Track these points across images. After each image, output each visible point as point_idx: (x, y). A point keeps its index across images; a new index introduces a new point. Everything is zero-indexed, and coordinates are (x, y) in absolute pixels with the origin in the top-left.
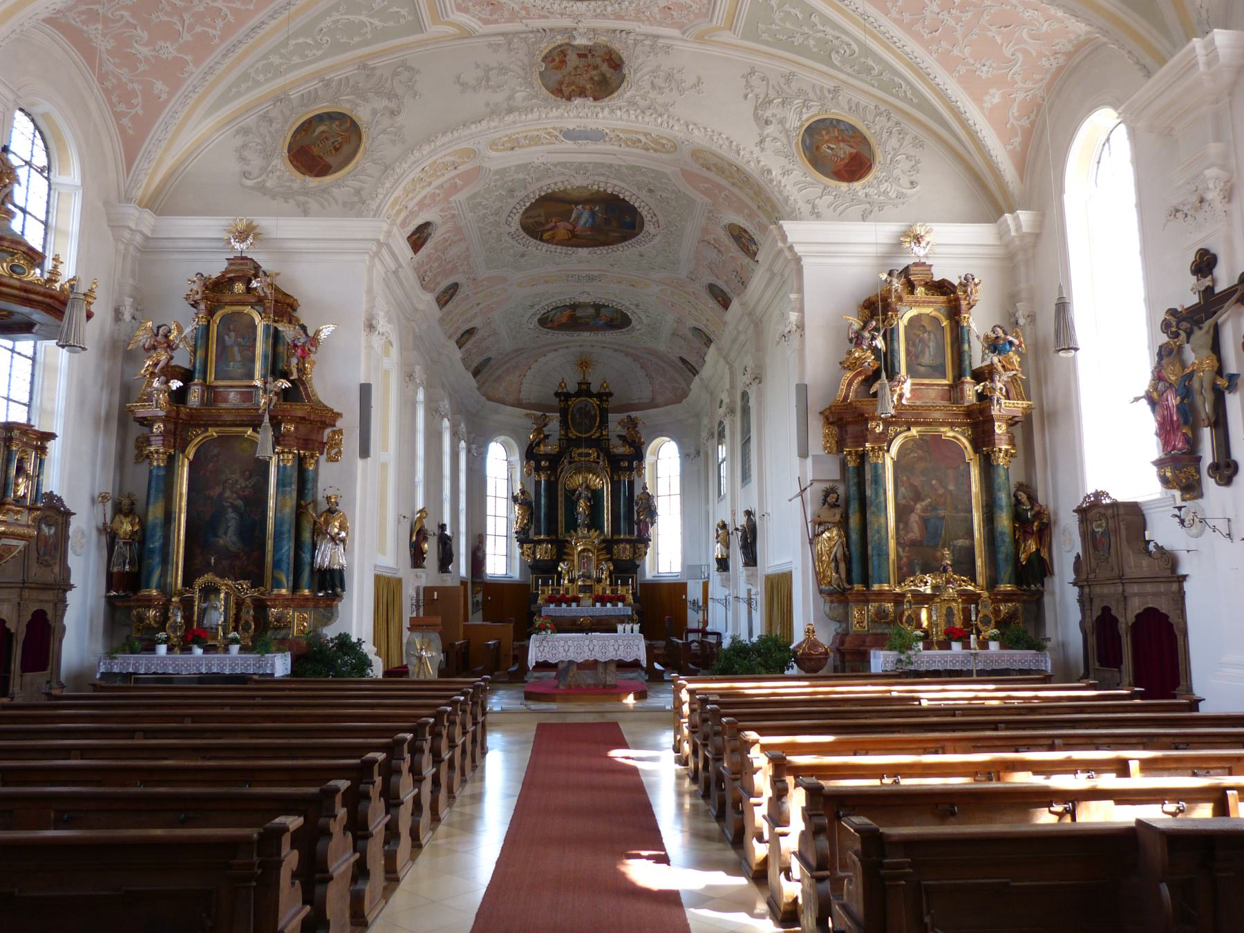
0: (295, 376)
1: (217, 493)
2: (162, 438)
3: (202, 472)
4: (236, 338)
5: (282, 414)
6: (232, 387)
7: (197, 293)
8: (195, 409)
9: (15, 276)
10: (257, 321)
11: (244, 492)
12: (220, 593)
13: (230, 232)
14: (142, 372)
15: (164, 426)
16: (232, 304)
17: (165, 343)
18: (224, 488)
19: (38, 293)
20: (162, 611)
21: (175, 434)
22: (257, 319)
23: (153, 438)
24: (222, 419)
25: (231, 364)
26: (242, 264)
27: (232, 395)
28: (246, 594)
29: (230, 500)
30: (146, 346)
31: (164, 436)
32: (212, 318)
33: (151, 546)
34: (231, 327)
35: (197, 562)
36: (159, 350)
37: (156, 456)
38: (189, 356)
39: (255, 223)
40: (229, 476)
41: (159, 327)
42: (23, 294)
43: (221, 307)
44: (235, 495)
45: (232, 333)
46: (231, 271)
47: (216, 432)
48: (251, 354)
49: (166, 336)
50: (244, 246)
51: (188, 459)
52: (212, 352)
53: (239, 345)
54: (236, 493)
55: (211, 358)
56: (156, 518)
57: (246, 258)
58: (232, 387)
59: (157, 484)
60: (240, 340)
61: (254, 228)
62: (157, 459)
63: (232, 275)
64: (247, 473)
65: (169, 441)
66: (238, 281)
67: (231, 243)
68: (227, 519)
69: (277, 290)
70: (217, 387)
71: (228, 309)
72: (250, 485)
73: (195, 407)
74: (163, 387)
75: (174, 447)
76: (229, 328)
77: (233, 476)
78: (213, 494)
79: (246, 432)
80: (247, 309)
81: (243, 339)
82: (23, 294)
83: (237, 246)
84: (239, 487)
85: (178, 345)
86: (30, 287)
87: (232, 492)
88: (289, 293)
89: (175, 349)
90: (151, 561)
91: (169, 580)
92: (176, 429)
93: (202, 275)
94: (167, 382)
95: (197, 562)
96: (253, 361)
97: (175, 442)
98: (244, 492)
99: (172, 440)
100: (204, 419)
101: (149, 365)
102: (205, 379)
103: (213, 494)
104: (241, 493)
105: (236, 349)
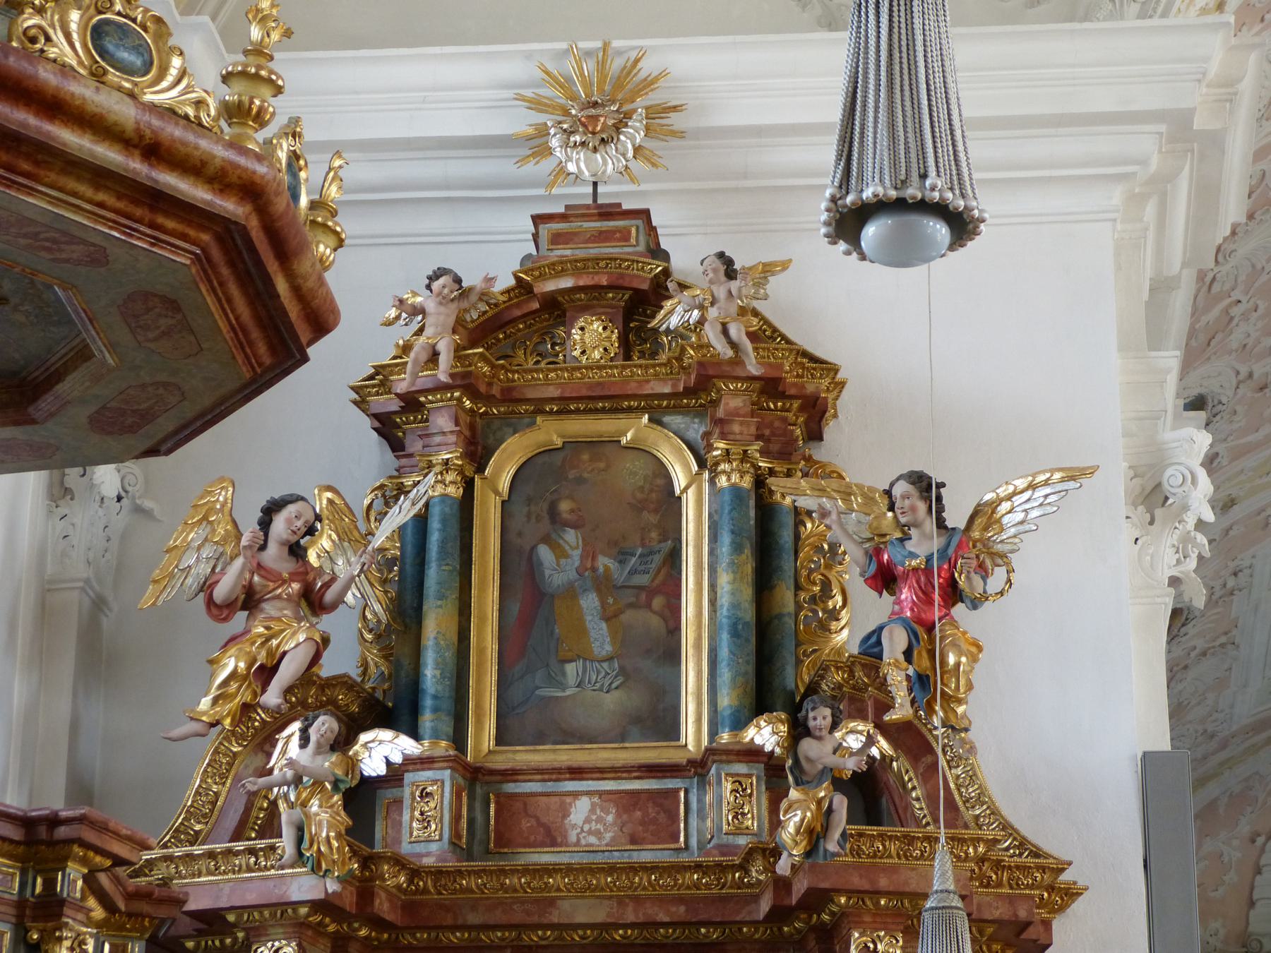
0: (901, 711)
4: (590, 554)
5: (857, 882)
6: (577, 773)
7: (434, 356)
8: (438, 873)
9: (113, 76)
10: (680, 479)
13: (537, 104)
14: (205, 703)
16: (565, 406)
17: (294, 577)
19: (194, 168)
22: (680, 472)
25: (571, 669)
26: (602, 237)
27: (580, 811)
30: (220, 593)
32: (481, 469)
34: (564, 506)
36: (269, 608)
38: (358, 649)
39: (648, 67)
41: (271, 510)
42: (136, 166)
43: (514, 424)
45: (571, 536)
46: (559, 269)
48: (655, 622)
49: (296, 551)
50: (608, 162)
52: (483, 619)
53: (603, 585)
55: (481, 651)
57: (610, 212)
58: (577, 773)
60: (604, 562)
61: (649, 84)
63: (567, 283)
66: (585, 309)
67: (549, 151)
69: (765, 335)
70: (512, 774)
71: (550, 432)
73: (428, 861)
74: (330, 763)
76: (553, 513)
80: (634, 429)
81: (622, 556)
82: (136, 166)
83: (579, 163)
85: (340, 600)
86: (175, 132)
88: (819, 353)
89: (333, 607)
93: (458, 280)
94: (342, 742)
96: (672, 655)
100: (473, 919)
101: (233, 675)
102: (459, 740)
105: (590, 602)
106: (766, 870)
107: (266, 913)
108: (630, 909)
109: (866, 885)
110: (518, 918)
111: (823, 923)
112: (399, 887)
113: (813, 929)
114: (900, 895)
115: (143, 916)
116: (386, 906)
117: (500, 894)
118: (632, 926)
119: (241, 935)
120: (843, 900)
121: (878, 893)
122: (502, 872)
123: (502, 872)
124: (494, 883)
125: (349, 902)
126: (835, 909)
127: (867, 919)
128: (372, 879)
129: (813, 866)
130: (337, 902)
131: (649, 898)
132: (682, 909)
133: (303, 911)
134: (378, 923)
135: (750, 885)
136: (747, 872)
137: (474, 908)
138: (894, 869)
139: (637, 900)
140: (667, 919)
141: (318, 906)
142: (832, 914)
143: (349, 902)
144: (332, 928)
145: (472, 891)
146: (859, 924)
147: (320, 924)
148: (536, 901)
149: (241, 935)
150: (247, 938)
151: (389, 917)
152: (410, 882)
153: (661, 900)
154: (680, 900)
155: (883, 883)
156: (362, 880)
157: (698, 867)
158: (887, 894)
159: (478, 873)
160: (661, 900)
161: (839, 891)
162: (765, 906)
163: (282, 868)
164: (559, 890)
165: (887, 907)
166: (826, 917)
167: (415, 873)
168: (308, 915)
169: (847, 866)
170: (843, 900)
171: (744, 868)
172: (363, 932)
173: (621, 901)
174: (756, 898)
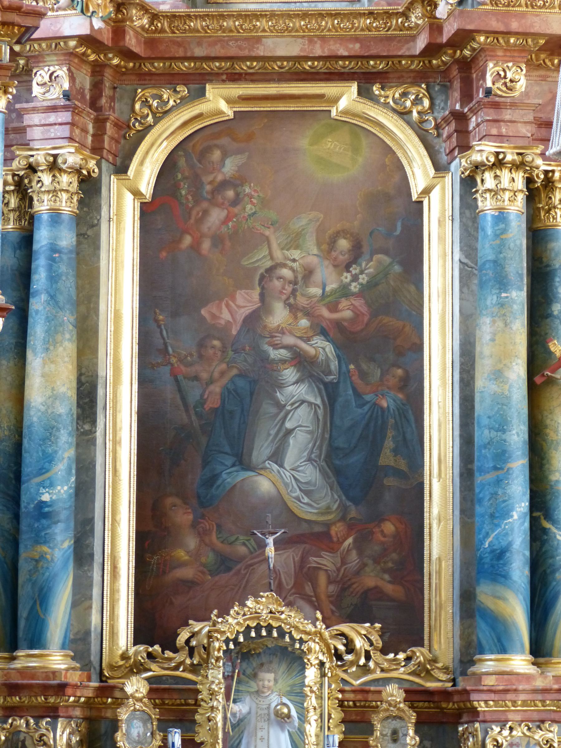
1: (242, 314)
2: (66, 116)
3: (188, 240)
5: (495, 25)
8: (173, 17)
11: (333, 307)
12: (303, 668)
15: (72, 78)
18: (262, 296)
20: (83, 728)
21: (94, 104)
23: (35, 119)
24: (261, 52)
28: (365, 669)
29: (289, 340)
31: (74, 110)
33: (46, 497)
35: (181, 554)
37: (46, 178)
40: (278, 255)
44: (304, 322)
47: (229, 101)
51: (136, 193)
54: (308, 314)
56: (55, 397)
59: (53, 278)
62: (54, 192)
64: (344, 244)
65: (85, 131)
68: (280, 407)
72: (354, 287)
75: (97, 149)
77: (296, 254)
78: (226, 315)
79: (335, 100)
84: (315, 291)
87: (293, 309)
90: (45, 549)
91: (95, 618)
92: (97, 87)
95: (181, 554)
97: (98, 136)
98: (333, 307)
99: (90, 128)
100: (199, 52)
103: (226, 315)
104: (325, 313)
106: (424, 16)
107: (44, 45)
108: (318, 46)
109: (501, 27)
110: (233, 51)
111: (465, 57)
112: (142, 27)
113: (457, 61)
114: (525, 35)
115: (13, 24)
116: (134, 41)
117: (220, 33)
118: (319, 58)
119: (22, 62)
120: (482, 39)
121: (508, 33)
122: (222, 16)
123: (222, 16)
124: (215, 25)
125: (107, 38)
126: (475, 45)
127: (500, 53)
128: (123, 21)
129: (462, 12)
130: (99, 38)
131: (332, 37)
132: (357, 46)
133: (72, 43)
134: (128, 54)
135: (410, 28)
136: (407, 18)
137: (199, 44)
138: (523, 15)
139: (323, 38)
140: (346, 54)
141: (84, 40)
142: (474, 50)
143: (107, 38)
144: (92, 57)
145: (198, 31)
146: (493, 57)
147: (84, 54)
148: (246, 39)
149: (22, 62)
150: (27, 64)
151: (136, 50)
152: (151, 23)
153: (342, 39)
154: (356, 39)
155: (514, 26)
156: (116, 21)
157: (371, 14)
158: (516, 34)
159: (202, 17)
160: (342, 39)
161: (478, 32)
162: (421, 43)
163: (59, 9)
164: (264, 31)
165: (515, 45)
166: (467, 53)
167: (155, 17)
168: (76, 47)
169: (487, 12)
170: (482, 39)
171: (405, 15)
172: (115, 61)
173: (311, 40)
174: (413, 38)
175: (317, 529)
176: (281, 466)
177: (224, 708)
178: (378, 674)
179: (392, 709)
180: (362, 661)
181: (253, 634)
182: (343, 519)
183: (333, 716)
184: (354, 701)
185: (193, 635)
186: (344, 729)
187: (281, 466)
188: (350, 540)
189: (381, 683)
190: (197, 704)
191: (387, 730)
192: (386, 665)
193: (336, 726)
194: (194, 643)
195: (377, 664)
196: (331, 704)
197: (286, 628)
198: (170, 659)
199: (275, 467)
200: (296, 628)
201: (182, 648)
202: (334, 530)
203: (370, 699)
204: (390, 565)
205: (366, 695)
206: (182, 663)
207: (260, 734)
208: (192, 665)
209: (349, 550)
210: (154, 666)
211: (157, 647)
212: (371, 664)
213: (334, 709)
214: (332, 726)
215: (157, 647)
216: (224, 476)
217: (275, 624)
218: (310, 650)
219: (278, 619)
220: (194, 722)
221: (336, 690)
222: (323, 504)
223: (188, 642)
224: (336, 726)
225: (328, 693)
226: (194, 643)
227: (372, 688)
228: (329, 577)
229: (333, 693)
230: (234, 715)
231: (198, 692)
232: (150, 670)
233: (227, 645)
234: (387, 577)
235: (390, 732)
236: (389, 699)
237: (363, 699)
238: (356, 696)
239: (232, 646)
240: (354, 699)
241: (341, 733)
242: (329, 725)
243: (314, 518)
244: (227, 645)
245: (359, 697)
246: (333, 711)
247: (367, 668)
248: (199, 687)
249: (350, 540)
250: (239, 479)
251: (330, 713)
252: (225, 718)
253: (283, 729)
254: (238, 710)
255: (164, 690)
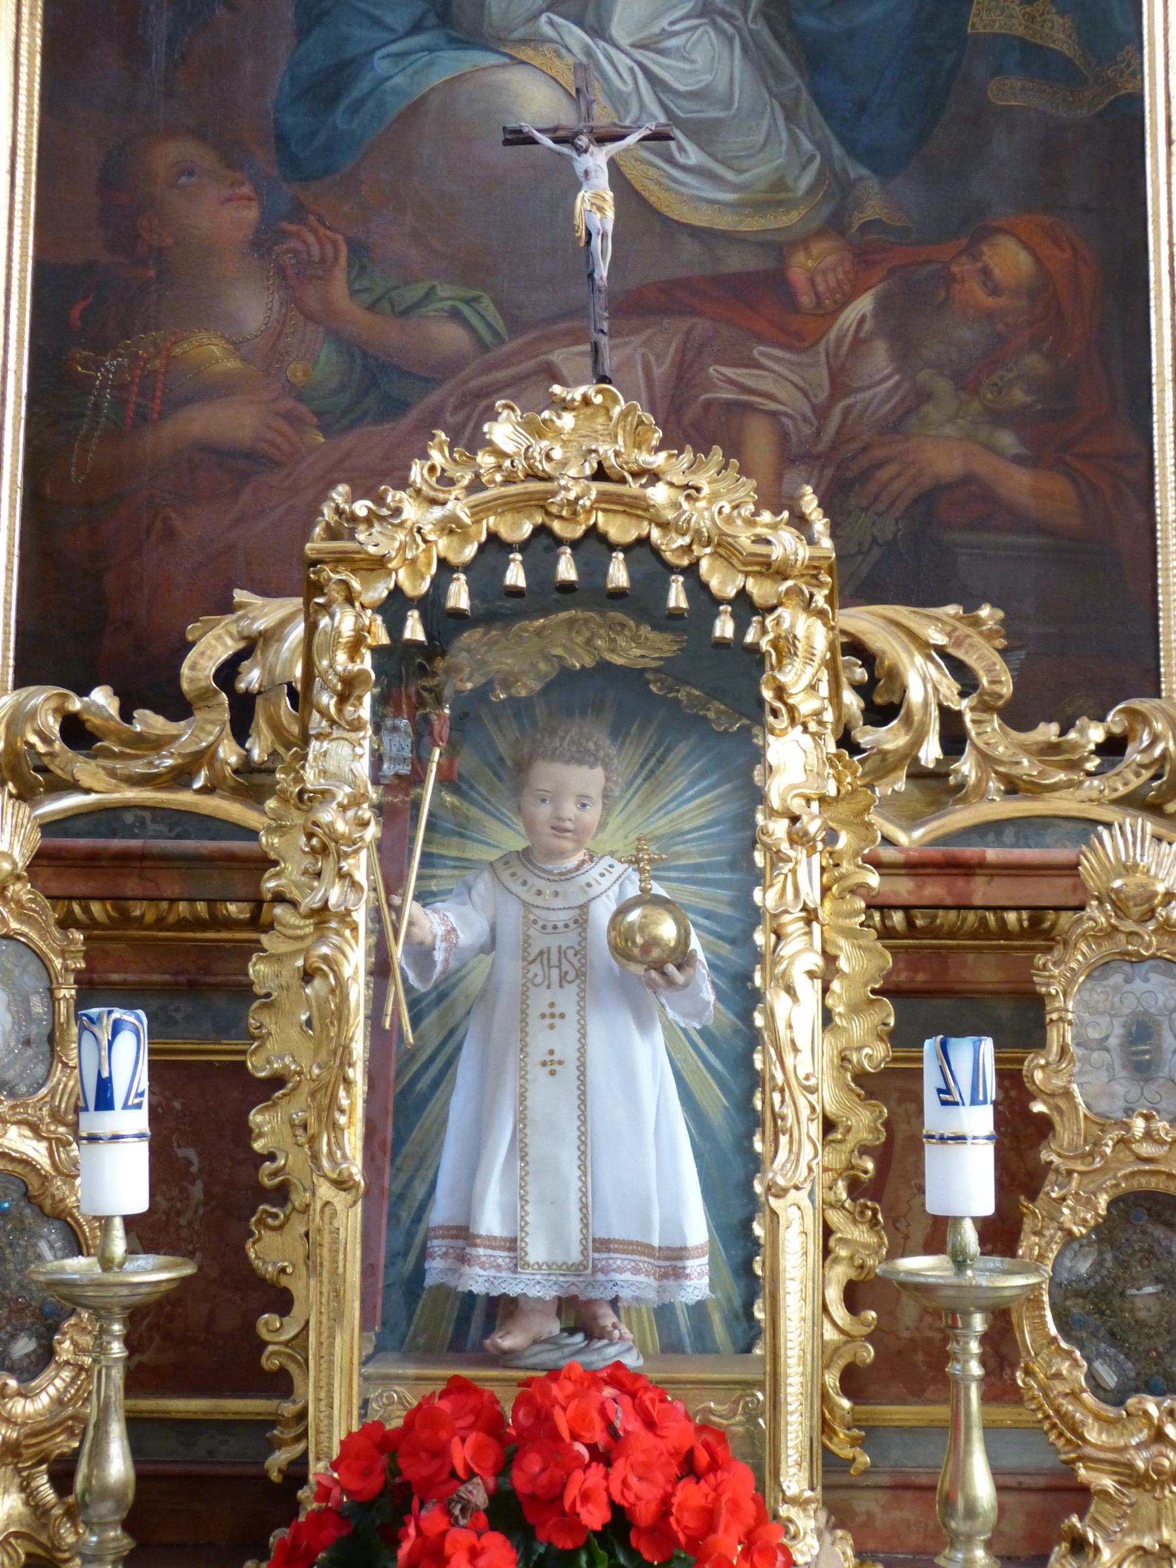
175: (736, 262)
176: (599, 31)
177: (376, 915)
178: (999, 807)
179: (1129, 926)
180: (931, 752)
181: (515, 576)
182: (835, 225)
183: (843, 964)
184: (906, 909)
185: (250, 647)
186: (892, 1021)
187: (599, 31)
188: (864, 304)
189: (1009, 834)
190: (258, 922)
191: (1104, 1021)
192: (1027, 766)
193: (855, 1009)
194: (252, 677)
195: (986, 759)
196: (836, 914)
197: (671, 545)
198: (156, 744)
199: (576, 36)
200: (724, 549)
201: (205, 695)
202: (800, 267)
203: (978, 901)
204: (1019, 396)
205: (960, 883)
206: (205, 756)
207: (541, 1041)
208: (247, 768)
209: (858, 342)
210: (85, 769)
211: (103, 698)
212: (967, 767)
213: (848, 933)
214: (840, 1009)
215: (103, 698)
216: (380, 65)
217: (619, 530)
218: (785, 647)
219: (637, 508)
220: (244, 992)
221: (857, 853)
222: (759, 171)
223: (228, 673)
224: (855, 1009)
225: (823, 870)
226: (252, 677)
227: (992, 854)
228: (784, 437)
229: (846, 867)
230: (421, 954)
231: (264, 863)
232: (74, 787)
233: (395, 626)
234: (1007, 440)
235: (1118, 1031)
236: (1117, 884)
237: (949, 901)
238: (920, 887)
239: (414, 630)
240: (913, 901)
241: (880, 1038)
242: (830, 1002)
243: (725, 222)
244: (395, 626)
245: (935, 890)
246: (842, 942)
247: (952, 780)
248: (269, 842)
249: (864, 304)
250: (437, 78)
251: (831, 950)
252: (381, 969)
253: (643, 1023)
254: (440, 930)
255: (124, 858)
